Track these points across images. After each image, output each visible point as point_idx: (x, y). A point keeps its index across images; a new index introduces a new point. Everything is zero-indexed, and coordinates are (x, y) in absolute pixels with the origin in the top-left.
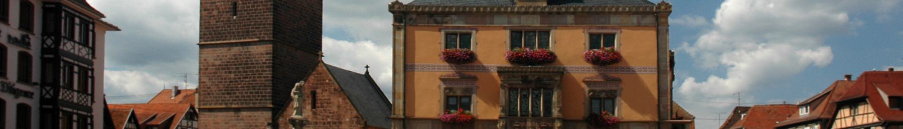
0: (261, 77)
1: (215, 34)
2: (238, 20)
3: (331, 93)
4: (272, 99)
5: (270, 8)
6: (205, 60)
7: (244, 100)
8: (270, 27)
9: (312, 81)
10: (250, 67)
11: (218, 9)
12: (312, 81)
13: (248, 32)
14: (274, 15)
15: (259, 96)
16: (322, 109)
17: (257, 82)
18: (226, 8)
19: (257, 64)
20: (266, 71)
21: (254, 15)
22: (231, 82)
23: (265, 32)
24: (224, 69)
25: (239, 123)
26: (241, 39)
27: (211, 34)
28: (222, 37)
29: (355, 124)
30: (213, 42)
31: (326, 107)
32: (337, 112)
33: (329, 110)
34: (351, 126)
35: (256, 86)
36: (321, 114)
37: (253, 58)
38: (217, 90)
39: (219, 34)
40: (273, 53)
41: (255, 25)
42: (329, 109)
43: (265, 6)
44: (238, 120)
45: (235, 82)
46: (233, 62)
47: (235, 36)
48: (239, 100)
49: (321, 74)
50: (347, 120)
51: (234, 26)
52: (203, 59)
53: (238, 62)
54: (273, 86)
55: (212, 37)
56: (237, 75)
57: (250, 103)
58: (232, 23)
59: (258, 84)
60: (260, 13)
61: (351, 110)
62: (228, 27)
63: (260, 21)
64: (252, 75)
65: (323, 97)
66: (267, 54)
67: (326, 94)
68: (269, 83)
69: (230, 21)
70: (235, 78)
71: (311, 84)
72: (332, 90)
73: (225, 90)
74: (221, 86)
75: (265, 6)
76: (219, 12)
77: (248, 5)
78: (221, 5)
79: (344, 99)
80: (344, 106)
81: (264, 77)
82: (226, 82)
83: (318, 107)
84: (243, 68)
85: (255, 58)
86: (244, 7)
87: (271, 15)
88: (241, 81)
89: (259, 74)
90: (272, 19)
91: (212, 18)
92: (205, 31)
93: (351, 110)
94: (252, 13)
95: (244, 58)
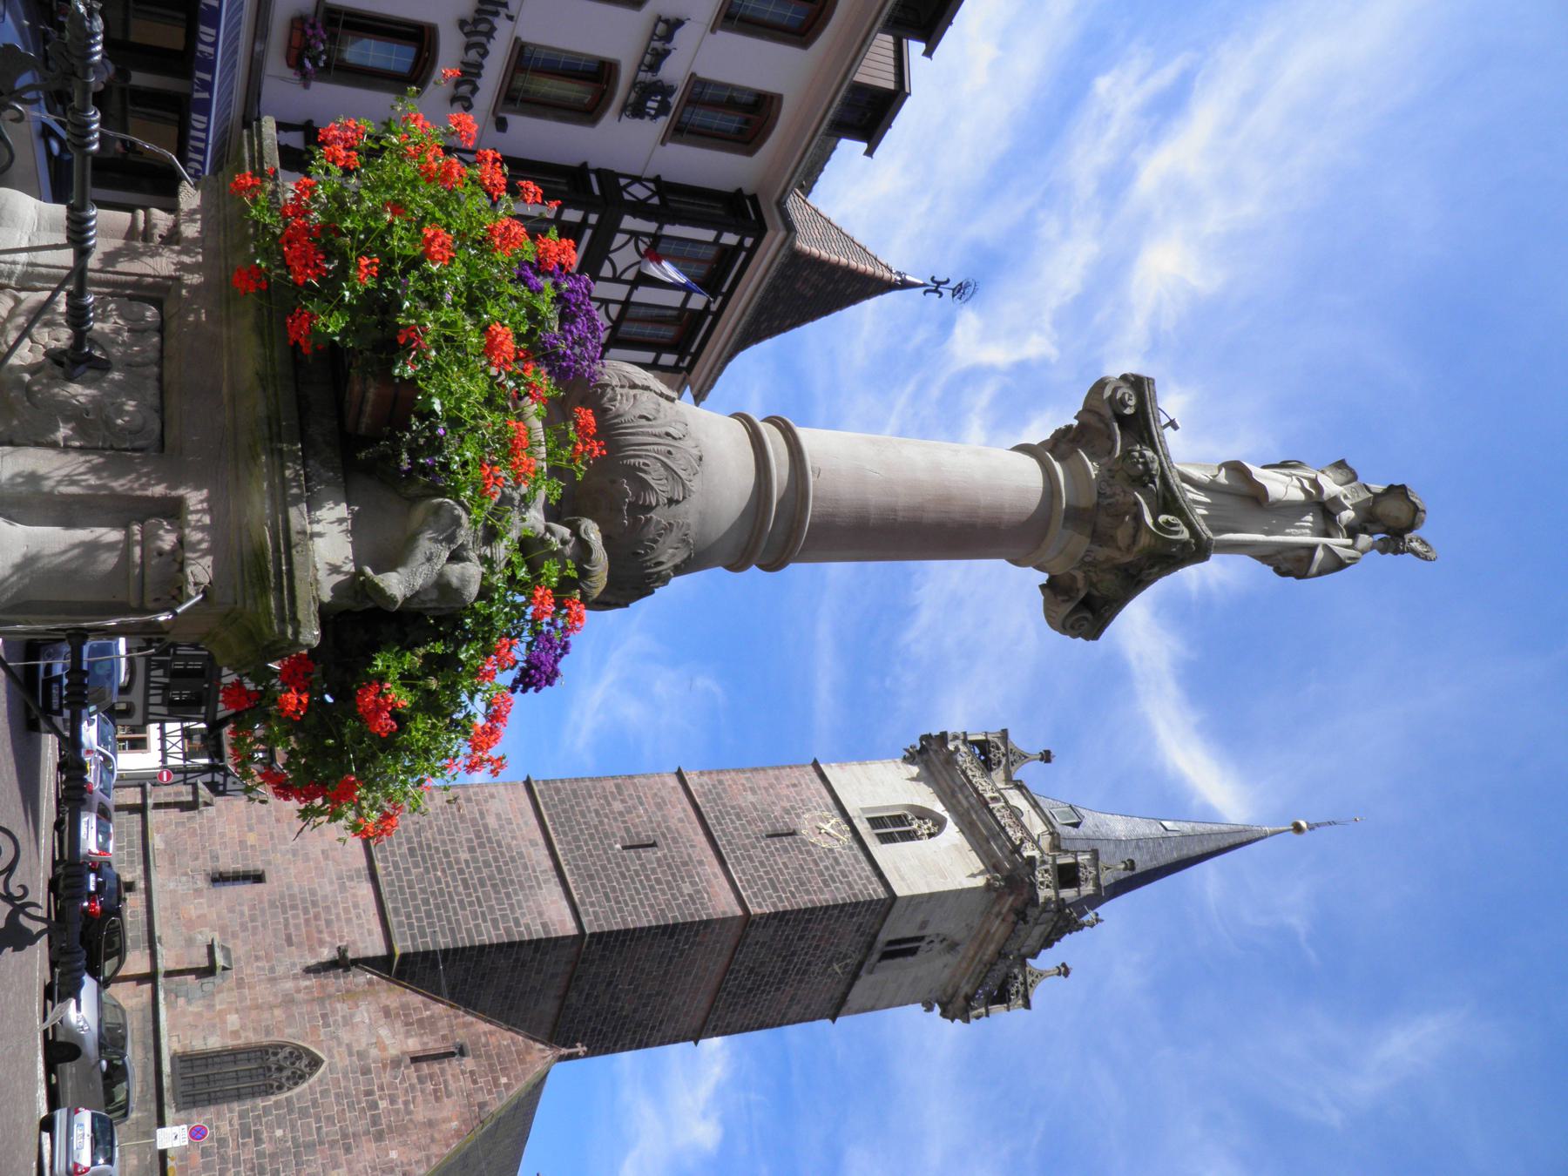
0: (476, 918)
1: (564, 811)
2: (614, 855)
4: (416, 954)
5: (664, 916)
6: (492, 796)
7: (401, 888)
8: (616, 923)
9: (493, 1040)
10: (497, 892)
11: (629, 812)
12: (493, 1040)
13: (591, 877)
14: (650, 928)
15: (419, 919)
16: (415, 1081)
17: (460, 912)
18: (635, 826)
19: (511, 906)
20: (496, 928)
21: (638, 886)
22: (446, 854)
23: (601, 915)
24: (478, 836)
25: (331, 883)
26: (568, 864)
27: (562, 801)
28: (562, 825)
30: (542, 808)
31: (422, 1091)
32: (411, 1120)
33: (414, 1098)
35: (447, 911)
36: (398, 1081)
39: (568, 819)
40: (549, 940)
41: (614, 890)
42: (420, 1099)
43: (668, 905)
44: (340, 878)
45: (449, 863)
46: (502, 854)
47: (571, 851)
48: (399, 877)
49: (522, 1061)
50: (393, 1155)
51: (596, 847)
52: (494, 790)
53: (506, 864)
54: (456, 950)
55: (555, 806)
56: (468, 867)
57: (395, 900)
58: (601, 842)
59: (456, 913)
60: (648, 899)
61: (428, 1159)
62: (592, 836)
63: (625, 901)
64: (478, 898)
65: (453, 1075)
66: (544, 925)
68: (462, 939)
69: (607, 837)
70: (458, 861)
71: (483, 1039)
72: (480, 1098)
73: (420, 843)
74: (429, 835)
75: (668, 905)
76: (621, 814)
77: (659, 870)
78: (639, 817)
79: (458, 1134)
80: (436, 1136)
81: (477, 926)
82: (444, 843)
83: (416, 1071)
84: (491, 878)
85: (527, 901)
86: (651, 863)
87: (649, 921)
88: (453, 875)
89: (483, 913)
90: (638, 925)
91: (602, 801)
92: (565, 789)
93: (428, 1159)
94: (641, 881)
95: (519, 876)
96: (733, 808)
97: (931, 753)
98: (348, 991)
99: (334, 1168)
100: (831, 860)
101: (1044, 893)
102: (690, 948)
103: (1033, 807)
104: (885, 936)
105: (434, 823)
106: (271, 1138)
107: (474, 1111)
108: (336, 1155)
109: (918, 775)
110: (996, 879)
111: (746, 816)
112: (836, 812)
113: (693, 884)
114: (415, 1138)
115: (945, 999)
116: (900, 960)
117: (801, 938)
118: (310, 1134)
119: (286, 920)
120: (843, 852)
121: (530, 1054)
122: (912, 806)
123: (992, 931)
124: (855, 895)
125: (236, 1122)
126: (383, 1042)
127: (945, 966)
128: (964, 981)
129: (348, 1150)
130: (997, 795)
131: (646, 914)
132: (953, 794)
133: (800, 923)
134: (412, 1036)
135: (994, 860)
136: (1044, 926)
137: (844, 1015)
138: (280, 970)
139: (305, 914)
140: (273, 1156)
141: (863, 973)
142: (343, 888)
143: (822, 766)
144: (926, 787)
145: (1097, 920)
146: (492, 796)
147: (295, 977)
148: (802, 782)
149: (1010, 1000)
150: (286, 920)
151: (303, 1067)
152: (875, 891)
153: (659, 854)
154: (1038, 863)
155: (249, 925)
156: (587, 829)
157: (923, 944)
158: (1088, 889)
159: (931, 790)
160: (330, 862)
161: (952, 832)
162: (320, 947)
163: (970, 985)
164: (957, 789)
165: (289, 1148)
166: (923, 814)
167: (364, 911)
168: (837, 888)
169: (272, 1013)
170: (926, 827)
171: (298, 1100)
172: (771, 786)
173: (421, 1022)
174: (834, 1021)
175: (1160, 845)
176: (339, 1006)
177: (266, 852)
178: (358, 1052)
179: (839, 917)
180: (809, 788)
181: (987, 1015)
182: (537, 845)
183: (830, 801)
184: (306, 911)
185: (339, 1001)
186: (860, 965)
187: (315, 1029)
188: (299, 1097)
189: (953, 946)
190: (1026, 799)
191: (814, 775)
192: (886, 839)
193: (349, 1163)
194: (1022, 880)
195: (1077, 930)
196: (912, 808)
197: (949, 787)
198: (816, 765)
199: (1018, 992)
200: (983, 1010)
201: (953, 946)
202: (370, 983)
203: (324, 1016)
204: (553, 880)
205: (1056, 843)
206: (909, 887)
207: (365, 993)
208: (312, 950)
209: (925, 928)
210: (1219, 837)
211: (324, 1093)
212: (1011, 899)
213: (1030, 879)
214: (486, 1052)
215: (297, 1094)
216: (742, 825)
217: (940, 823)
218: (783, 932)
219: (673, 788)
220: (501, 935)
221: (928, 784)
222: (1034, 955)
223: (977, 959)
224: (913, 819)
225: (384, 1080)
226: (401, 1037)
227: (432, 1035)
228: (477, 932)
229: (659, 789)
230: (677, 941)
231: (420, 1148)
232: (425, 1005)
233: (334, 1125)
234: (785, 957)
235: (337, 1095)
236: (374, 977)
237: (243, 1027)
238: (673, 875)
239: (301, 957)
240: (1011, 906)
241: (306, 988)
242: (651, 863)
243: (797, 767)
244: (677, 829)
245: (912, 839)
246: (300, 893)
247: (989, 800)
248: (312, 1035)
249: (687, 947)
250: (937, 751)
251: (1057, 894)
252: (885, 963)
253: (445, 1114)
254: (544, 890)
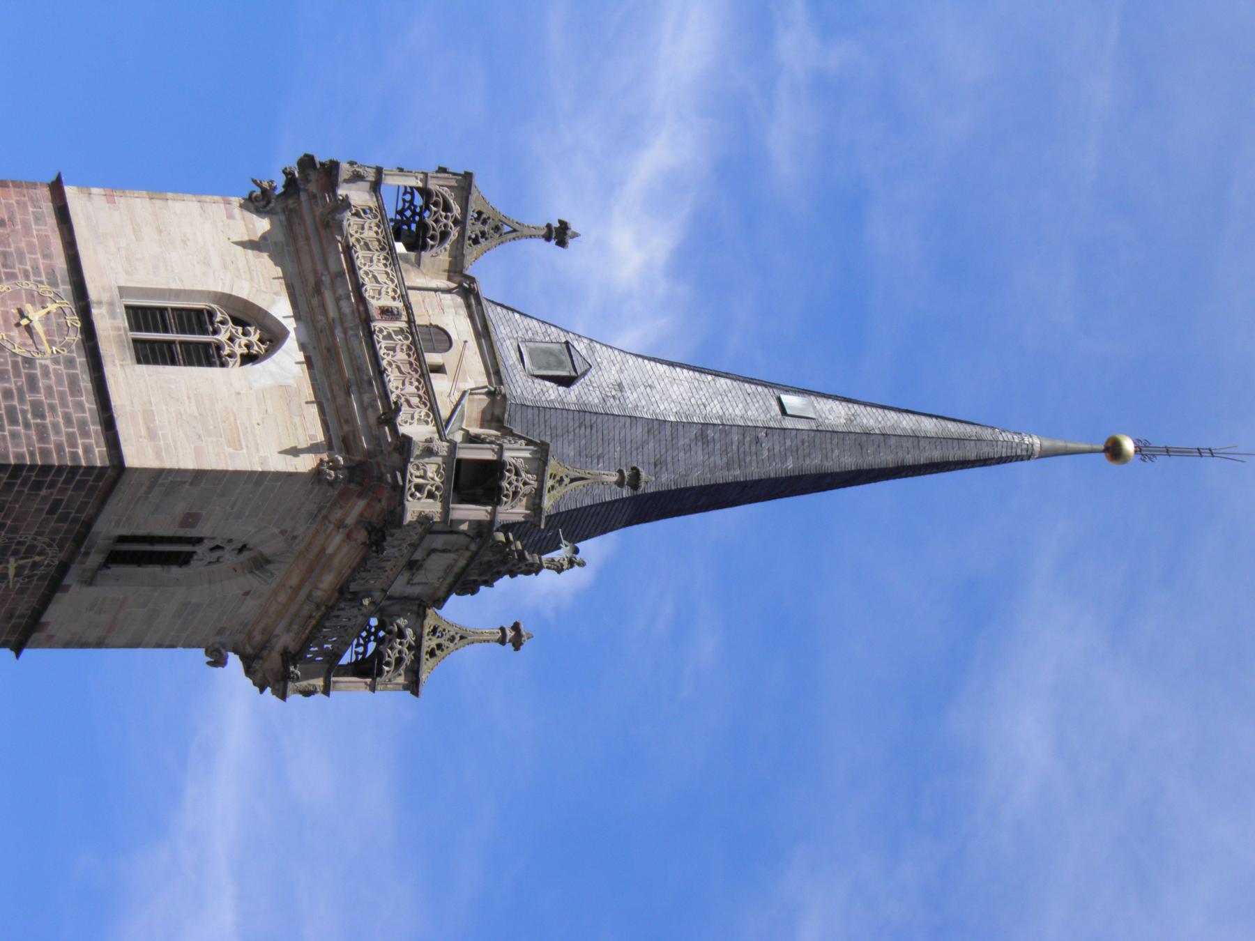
97: (303, 197)
100: (22, 381)
101: (416, 507)
103: (478, 335)
109: (264, 237)
110: (335, 467)
112: (65, 288)
115: (249, 650)
116: (156, 569)
120: (52, 367)
122: (230, 297)
123: (330, 550)
124: (45, 453)
127: (246, 593)
128: (283, 624)
130: (399, 304)
132: (318, 290)
135: (346, 428)
136: (450, 557)
137: (30, 647)
141: (70, 579)
143: (70, 191)
144: (270, 263)
145: (571, 563)
148: (18, 217)
149: (380, 673)
152: (87, 450)
154: (417, 452)
157: (200, 550)
158: (513, 511)
159: (278, 271)
161: (290, 358)
163: (292, 635)
164: (326, 279)
168: (14, 435)
170: (244, 340)
174: (18, 653)
175: (757, 440)
180: (27, 229)
181: (326, 691)
183: (60, 263)
186: (64, 568)
189: (260, 564)
190: (471, 317)
191: (47, 208)
192: (149, 354)
194: (381, 478)
195: (528, 573)
196: (226, 300)
197: (315, 272)
198: (57, 188)
199: (399, 661)
200: (319, 682)
201: (260, 564)
205: (497, 412)
206: (158, 455)
209: (193, 525)
210: (907, 444)
212: (360, 505)
213: (395, 477)
217: (273, 338)
221: (277, 259)
222: (439, 602)
223: (304, 592)
224: (222, 323)
240: (361, 515)
243: (17, 184)
245: (210, 364)
247: (375, 312)
250: (314, 196)
251: (446, 511)
252: (117, 570)
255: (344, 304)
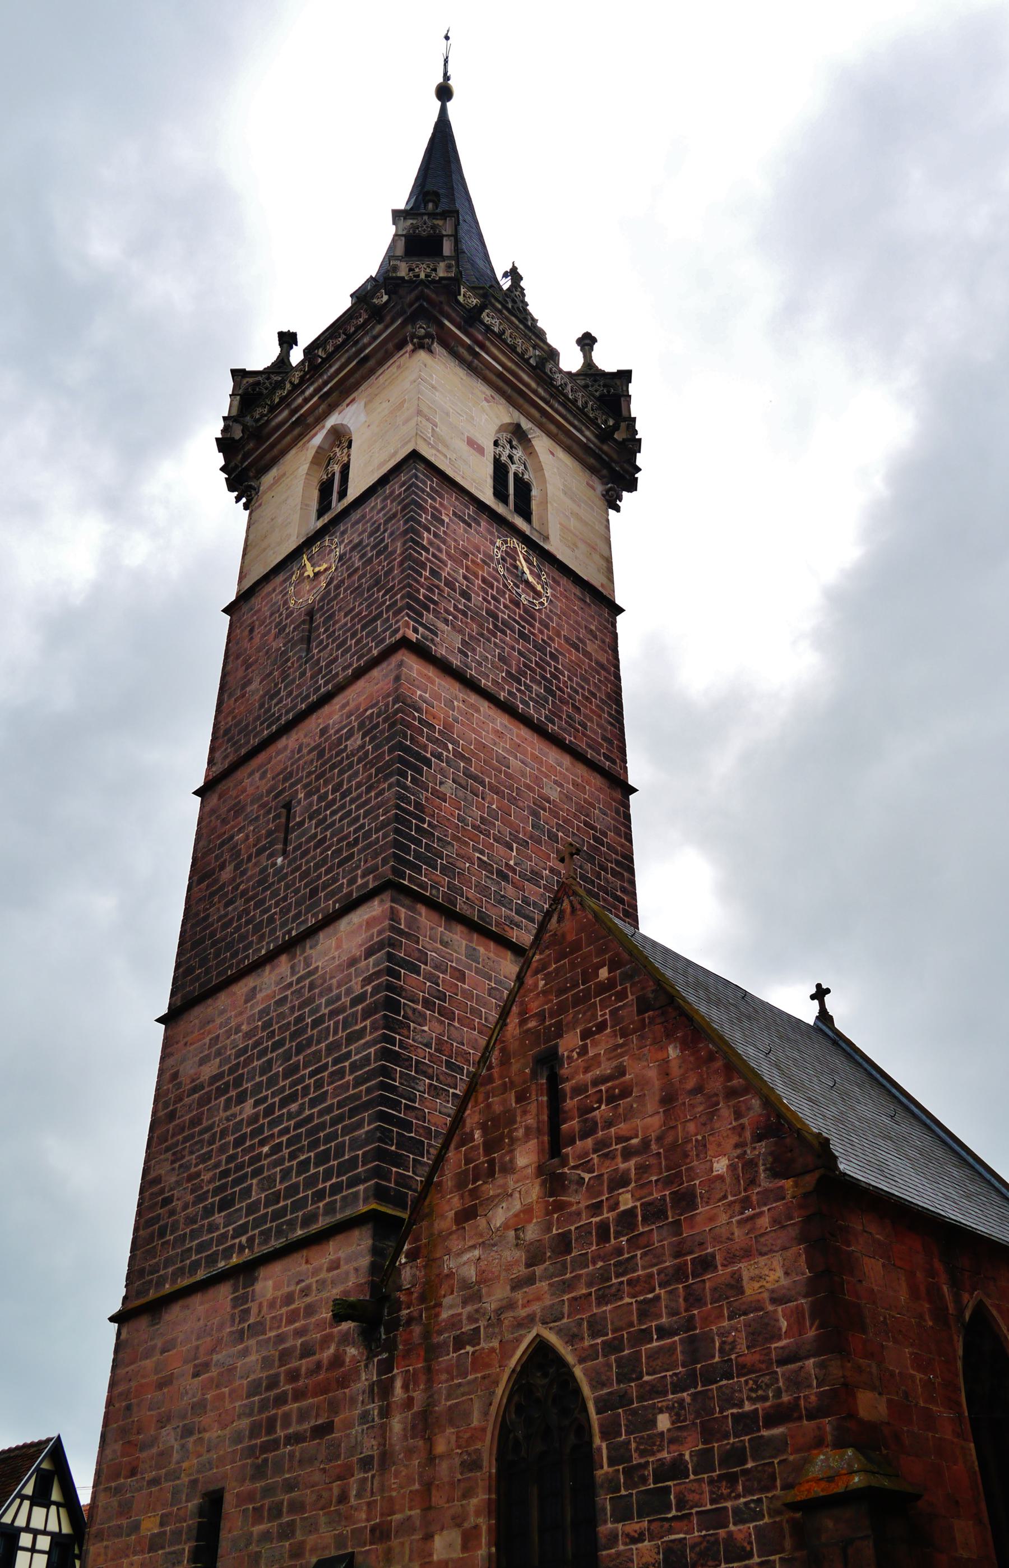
3: (624, 1034)
9: (535, 1007)
12: (535, 1007)
13: (314, 892)
15: (328, 1175)
16: (589, 1142)
18: (258, 840)
20: (361, 1033)
25: (245, 1353)
29: (765, 1182)
31: (609, 1124)
32: (659, 1139)
33: (620, 1139)
34: (746, 1203)
35: (322, 1126)
36: (587, 1176)
37: (321, 995)
38: (190, 1198)
42: (623, 1128)
45: (254, 1134)
48: (258, 1223)
50: (721, 1166)
56: (265, 1099)
57: (292, 1224)
59: (329, 1109)
65: (586, 1070)
67: (599, 1047)
68: (369, 1091)
69: (264, 880)
70: (254, 1119)
71: (532, 1024)
80: (691, 1083)
81: (354, 1066)
96: (262, 705)
98: (423, 1299)
99: (741, 1291)
102: (455, 743)
104: (487, 496)
105: (193, 1170)
106: (671, 1441)
107: (652, 1020)
108: (714, 1290)
111: (276, 685)
113: (350, 734)
114: (691, 1127)
117: (466, 595)
118: (671, 1349)
119: (290, 1440)
120: (346, 541)
121: (564, 936)
125: (634, 1527)
126: (516, 1215)
129: (706, 1264)
131: (377, 796)
133: (438, 587)
134: (512, 1161)
138: (370, 1446)
139: (285, 1402)
140: (708, 1433)
142: (257, 1329)
146: (175, 1076)
147: (385, 1412)
150: (290, 1440)
151: (546, 1381)
153: (301, 795)
155: (286, 1519)
156: (248, 914)
160: (215, 1357)
162: (342, 1364)
165: (694, 1396)
166: (322, 458)
167: (298, 1283)
168: (391, 534)
169: (441, 1457)
171: (604, 1385)
172: (245, 661)
173: (490, 1146)
174: (621, 610)
176: (445, 1315)
177: (176, 1492)
178: (528, 1265)
179: (436, 535)
182: (255, 988)
184: (281, 1400)
185: (437, 1315)
187: (478, 1361)
188: (597, 1383)
193: (731, 1258)
202: (413, 1256)
203: (459, 1343)
204: (308, 952)
207: (431, 1262)
208: (343, 1382)
211: (596, 1327)
214: (551, 1017)
215: (593, 1388)
216: (285, 687)
218: (447, 611)
219: (220, 798)
220: (372, 1023)
225: (582, 1205)
226: (511, 1181)
227: (515, 1122)
228: (364, 1066)
229: (217, 818)
230: (439, 757)
231: (712, 1114)
232: (462, 1143)
233: (658, 1298)
234: (495, 626)
235: (602, 1300)
236: (406, 1247)
237: (458, 1521)
238: (333, 768)
239: (353, 1401)
241: (405, 1387)
242: (311, 804)
244: (273, 779)
246: (251, 1414)
248: (488, 1366)
249: (450, 746)
253: (652, 1074)
254: (320, 964)
255: (307, 393)
